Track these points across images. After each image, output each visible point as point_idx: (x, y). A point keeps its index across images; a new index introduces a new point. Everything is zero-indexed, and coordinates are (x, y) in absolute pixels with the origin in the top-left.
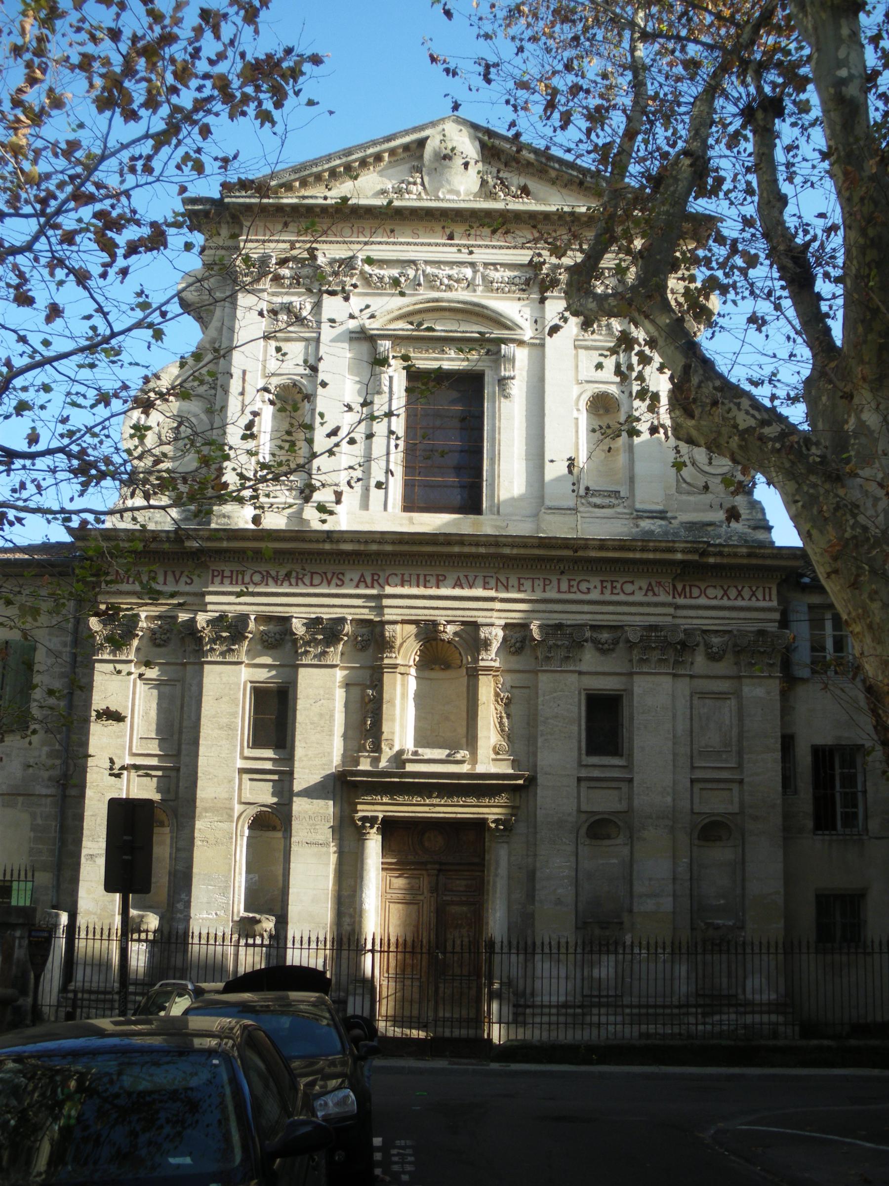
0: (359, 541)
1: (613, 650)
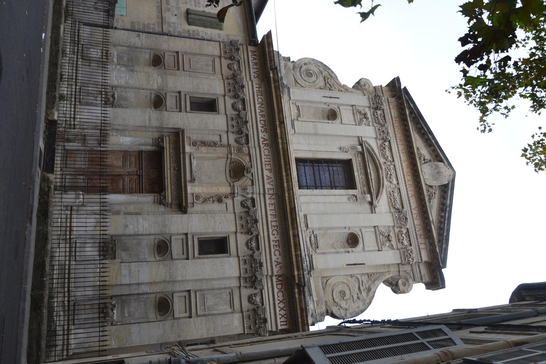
1: (248, 248)
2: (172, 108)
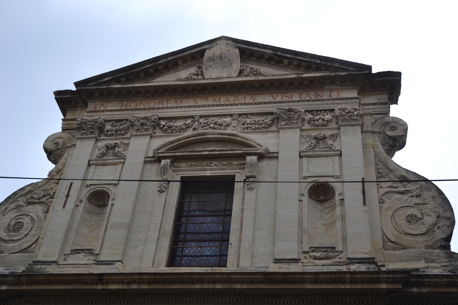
0: (123, 283)
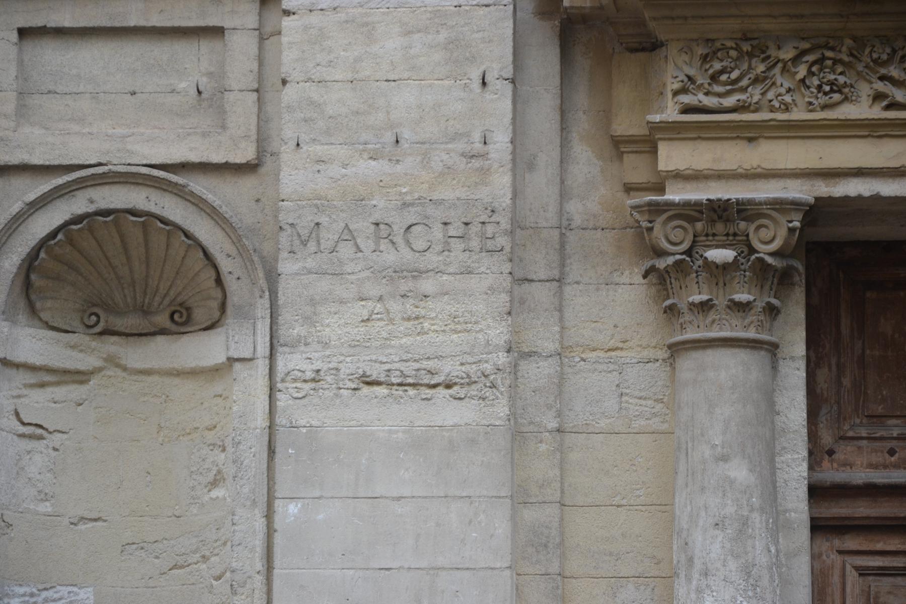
2: (210, 99)
